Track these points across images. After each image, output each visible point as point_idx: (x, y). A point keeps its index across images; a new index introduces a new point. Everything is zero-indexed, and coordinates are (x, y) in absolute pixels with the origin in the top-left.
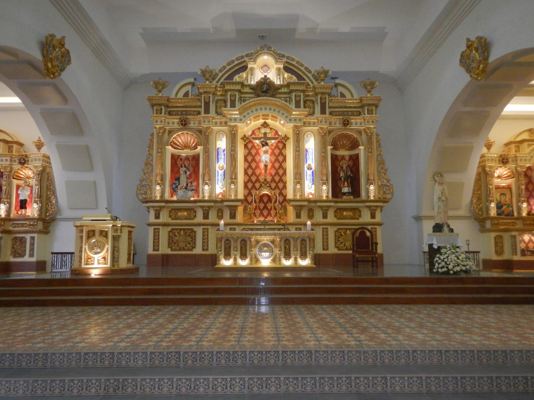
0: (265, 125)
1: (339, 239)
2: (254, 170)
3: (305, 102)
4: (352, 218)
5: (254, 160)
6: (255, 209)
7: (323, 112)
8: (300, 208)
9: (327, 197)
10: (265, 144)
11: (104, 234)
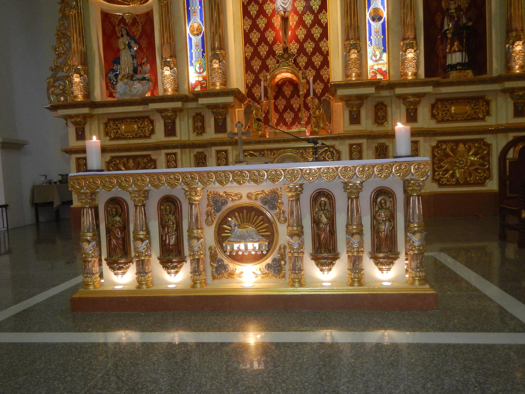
1: (442, 164)
2: (262, 33)
5: (261, 12)
8: (357, 102)
9: (415, 74)
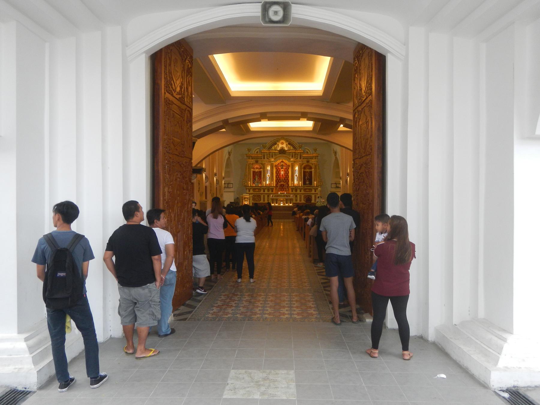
0: (282, 162)
2: (279, 176)
3: (295, 155)
4: (309, 192)
5: (279, 173)
6: (279, 188)
7: (300, 158)
9: (301, 185)
10: (282, 168)
11: (248, 198)
